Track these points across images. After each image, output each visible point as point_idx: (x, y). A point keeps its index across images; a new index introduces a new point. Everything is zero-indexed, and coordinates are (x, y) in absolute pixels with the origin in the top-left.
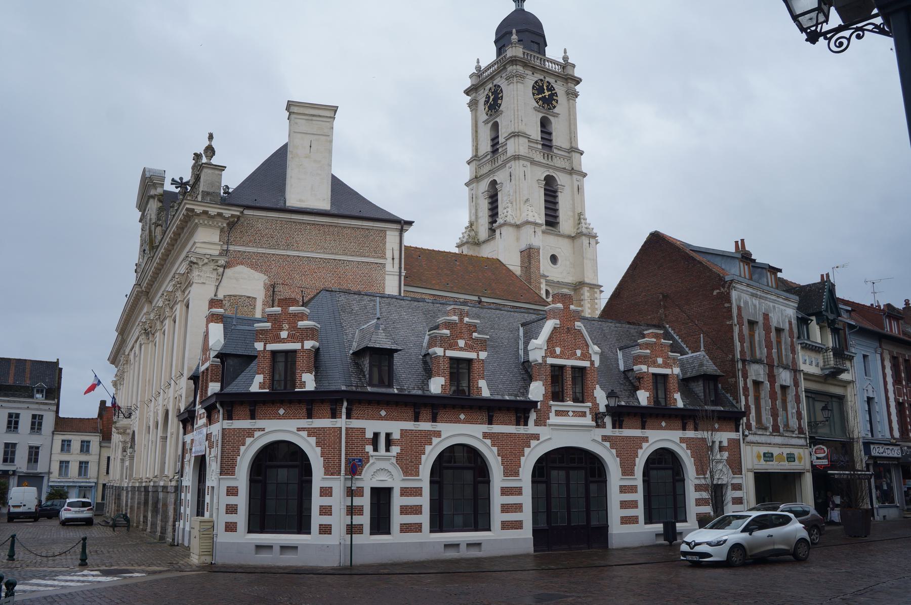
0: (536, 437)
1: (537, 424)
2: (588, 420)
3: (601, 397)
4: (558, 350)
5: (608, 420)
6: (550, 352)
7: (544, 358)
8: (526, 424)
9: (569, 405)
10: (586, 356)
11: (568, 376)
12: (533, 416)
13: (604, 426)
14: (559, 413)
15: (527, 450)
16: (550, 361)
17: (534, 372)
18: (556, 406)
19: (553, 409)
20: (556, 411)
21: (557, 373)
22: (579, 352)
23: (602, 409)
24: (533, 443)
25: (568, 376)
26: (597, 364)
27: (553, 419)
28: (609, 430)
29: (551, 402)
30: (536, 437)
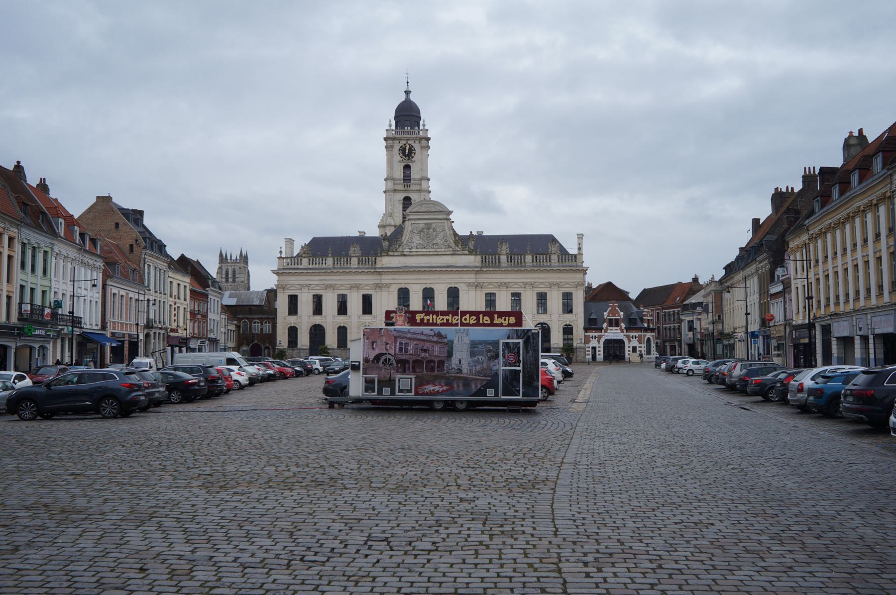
2: (619, 331)
3: (623, 325)
5: (625, 331)
6: (608, 316)
9: (614, 328)
10: (619, 316)
11: (614, 321)
12: (603, 331)
13: (623, 332)
14: (610, 330)
18: (610, 328)
21: (611, 320)
23: (623, 328)
25: (614, 321)
26: (622, 317)
27: (609, 331)
28: (625, 333)
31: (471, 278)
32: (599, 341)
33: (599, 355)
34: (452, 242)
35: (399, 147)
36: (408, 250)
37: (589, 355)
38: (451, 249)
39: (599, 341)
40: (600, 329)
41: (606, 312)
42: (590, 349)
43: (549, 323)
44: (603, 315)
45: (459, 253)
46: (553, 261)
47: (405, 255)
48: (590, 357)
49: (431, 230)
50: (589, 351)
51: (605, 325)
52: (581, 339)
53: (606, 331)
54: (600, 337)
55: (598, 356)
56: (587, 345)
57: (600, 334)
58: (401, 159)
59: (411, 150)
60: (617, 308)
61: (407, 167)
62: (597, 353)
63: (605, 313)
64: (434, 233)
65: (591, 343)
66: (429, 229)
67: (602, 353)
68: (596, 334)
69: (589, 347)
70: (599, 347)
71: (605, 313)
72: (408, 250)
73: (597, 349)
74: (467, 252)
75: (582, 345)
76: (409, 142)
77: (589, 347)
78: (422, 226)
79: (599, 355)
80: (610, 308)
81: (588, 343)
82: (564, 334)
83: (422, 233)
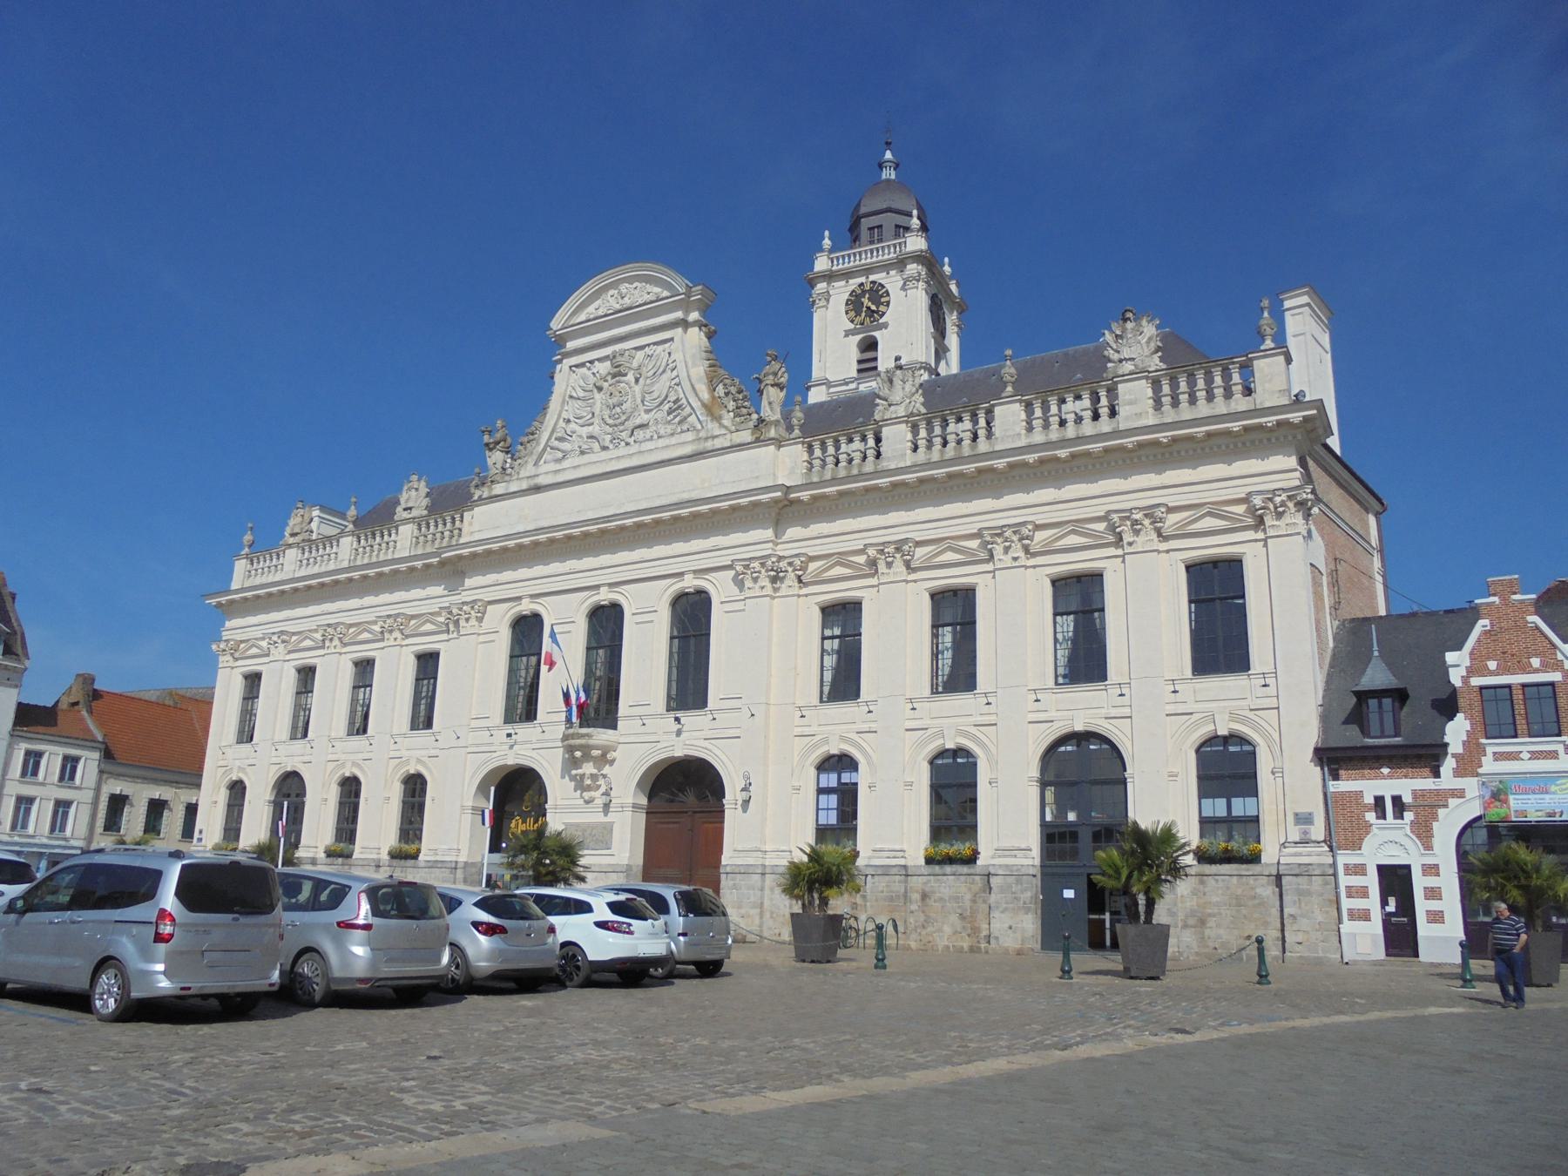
0: (1460, 794)
1: (1459, 773)
4: (1492, 665)
6: (1471, 671)
7: (1465, 680)
8: (1437, 774)
12: (1448, 765)
14: (1498, 757)
15: (1441, 812)
16: (1476, 681)
17: (1462, 702)
18: (1492, 747)
19: (1490, 750)
20: (1495, 753)
22: (1536, 662)
24: (1452, 802)
25: (1518, 696)
29: (1484, 741)
30: (1460, 794)
31: (755, 540)
32: (1424, 832)
33: (1436, 917)
34: (696, 404)
35: (846, 296)
36: (553, 467)
37: (1365, 916)
38: (690, 436)
39: (1424, 832)
40: (1428, 756)
41: (1458, 647)
42: (1372, 881)
43: (1118, 733)
44: (1444, 669)
45: (718, 443)
46: (1123, 411)
47: (537, 489)
48: (1376, 926)
49: (630, 377)
50: (1363, 892)
51: (1457, 731)
52: (1304, 819)
53: (1468, 765)
54: (1429, 807)
55: (1424, 929)
56: (1344, 858)
57: (1426, 783)
58: (852, 326)
59: (878, 294)
60: (1534, 619)
61: (870, 345)
62: (1421, 906)
63: (1451, 657)
64: (637, 389)
65: (1369, 843)
66: (618, 374)
67: (1452, 903)
68: (1405, 785)
69: (1360, 870)
70: (1430, 870)
71: (1451, 657)
72: (553, 467)
73: (1419, 883)
74: (746, 436)
75: (1317, 856)
76: (872, 278)
77: (1360, 870)
78: (604, 368)
79: (1436, 917)
80: (1482, 624)
81: (1356, 845)
82: (1203, 794)
83: (598, 396)
